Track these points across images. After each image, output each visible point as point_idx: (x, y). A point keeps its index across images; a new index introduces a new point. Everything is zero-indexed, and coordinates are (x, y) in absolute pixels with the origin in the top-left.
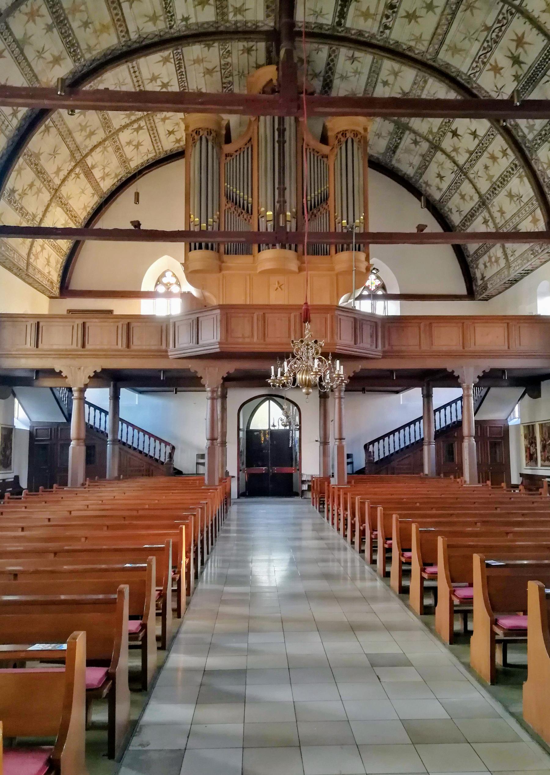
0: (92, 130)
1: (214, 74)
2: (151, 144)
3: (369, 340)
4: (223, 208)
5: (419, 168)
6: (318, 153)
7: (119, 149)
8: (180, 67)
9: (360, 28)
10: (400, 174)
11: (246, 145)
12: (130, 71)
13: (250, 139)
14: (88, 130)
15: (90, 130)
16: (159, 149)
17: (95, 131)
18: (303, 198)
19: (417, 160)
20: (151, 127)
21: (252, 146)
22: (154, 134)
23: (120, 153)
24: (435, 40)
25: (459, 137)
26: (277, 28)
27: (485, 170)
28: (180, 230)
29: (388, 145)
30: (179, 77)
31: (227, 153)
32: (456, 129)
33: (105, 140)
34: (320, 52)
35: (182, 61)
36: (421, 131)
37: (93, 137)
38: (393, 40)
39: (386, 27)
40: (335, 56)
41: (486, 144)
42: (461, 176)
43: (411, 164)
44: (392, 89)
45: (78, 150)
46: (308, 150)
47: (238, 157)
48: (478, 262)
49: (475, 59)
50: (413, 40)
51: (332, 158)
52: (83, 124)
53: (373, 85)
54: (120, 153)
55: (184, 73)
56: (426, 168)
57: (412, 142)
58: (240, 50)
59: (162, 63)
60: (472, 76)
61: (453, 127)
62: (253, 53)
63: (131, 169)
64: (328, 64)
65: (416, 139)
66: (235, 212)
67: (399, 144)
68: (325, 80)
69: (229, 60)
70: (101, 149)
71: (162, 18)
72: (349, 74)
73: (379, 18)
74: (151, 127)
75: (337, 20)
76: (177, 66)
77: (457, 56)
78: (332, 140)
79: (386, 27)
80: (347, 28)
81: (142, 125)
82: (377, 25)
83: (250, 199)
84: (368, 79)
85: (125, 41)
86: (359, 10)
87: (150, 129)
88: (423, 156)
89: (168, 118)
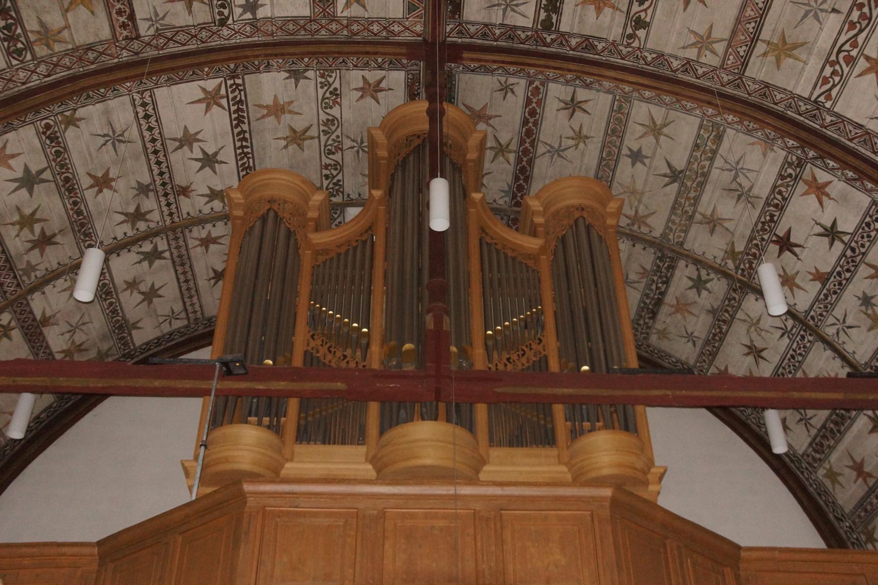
0: (48, 233)
1: (307, 143)
5: (707, 342)
7: (108, 293)
8: (240, 121)
9: (587, 32)
14: (37, 228)
15: (43, 231)
16: (195, 312)
19: (700, 325)
20: (180, 256)
22: (184, 273)
23: (111, 304)
25: (796, 250)
27: (863, 308)
30: (238, 144)
32: (789, 232)
35: (244, 107)
37: (49, 249)
38: (651, 52)
39: (640, 24)
40: (539, 103)
41: (863, 246)
42: (803, 337)
43: (690, 337)
45: (11, 269)
48: (870, 528)
49: (830, 55)
52: (28, 211)
54: (111, 304)
55: (247, 135)
56: (722, 340)
57: (691, 284)
59: (203, 106)
60: (822, 99)
61: (781, 232)
63: (135, 350)
64: (525, 122)
65: (699, 276)
67: (663, 294)
68: (519, 160)
69: (335, 111)
75: (543, 15)
79: (640, 24)
80: (563, 35)
81: (160, 249)
82: (620, 18)
84: (602, 151)
85: (126, 38)
87: (177, 260)
88: (713, 312)
89: (215, 241)
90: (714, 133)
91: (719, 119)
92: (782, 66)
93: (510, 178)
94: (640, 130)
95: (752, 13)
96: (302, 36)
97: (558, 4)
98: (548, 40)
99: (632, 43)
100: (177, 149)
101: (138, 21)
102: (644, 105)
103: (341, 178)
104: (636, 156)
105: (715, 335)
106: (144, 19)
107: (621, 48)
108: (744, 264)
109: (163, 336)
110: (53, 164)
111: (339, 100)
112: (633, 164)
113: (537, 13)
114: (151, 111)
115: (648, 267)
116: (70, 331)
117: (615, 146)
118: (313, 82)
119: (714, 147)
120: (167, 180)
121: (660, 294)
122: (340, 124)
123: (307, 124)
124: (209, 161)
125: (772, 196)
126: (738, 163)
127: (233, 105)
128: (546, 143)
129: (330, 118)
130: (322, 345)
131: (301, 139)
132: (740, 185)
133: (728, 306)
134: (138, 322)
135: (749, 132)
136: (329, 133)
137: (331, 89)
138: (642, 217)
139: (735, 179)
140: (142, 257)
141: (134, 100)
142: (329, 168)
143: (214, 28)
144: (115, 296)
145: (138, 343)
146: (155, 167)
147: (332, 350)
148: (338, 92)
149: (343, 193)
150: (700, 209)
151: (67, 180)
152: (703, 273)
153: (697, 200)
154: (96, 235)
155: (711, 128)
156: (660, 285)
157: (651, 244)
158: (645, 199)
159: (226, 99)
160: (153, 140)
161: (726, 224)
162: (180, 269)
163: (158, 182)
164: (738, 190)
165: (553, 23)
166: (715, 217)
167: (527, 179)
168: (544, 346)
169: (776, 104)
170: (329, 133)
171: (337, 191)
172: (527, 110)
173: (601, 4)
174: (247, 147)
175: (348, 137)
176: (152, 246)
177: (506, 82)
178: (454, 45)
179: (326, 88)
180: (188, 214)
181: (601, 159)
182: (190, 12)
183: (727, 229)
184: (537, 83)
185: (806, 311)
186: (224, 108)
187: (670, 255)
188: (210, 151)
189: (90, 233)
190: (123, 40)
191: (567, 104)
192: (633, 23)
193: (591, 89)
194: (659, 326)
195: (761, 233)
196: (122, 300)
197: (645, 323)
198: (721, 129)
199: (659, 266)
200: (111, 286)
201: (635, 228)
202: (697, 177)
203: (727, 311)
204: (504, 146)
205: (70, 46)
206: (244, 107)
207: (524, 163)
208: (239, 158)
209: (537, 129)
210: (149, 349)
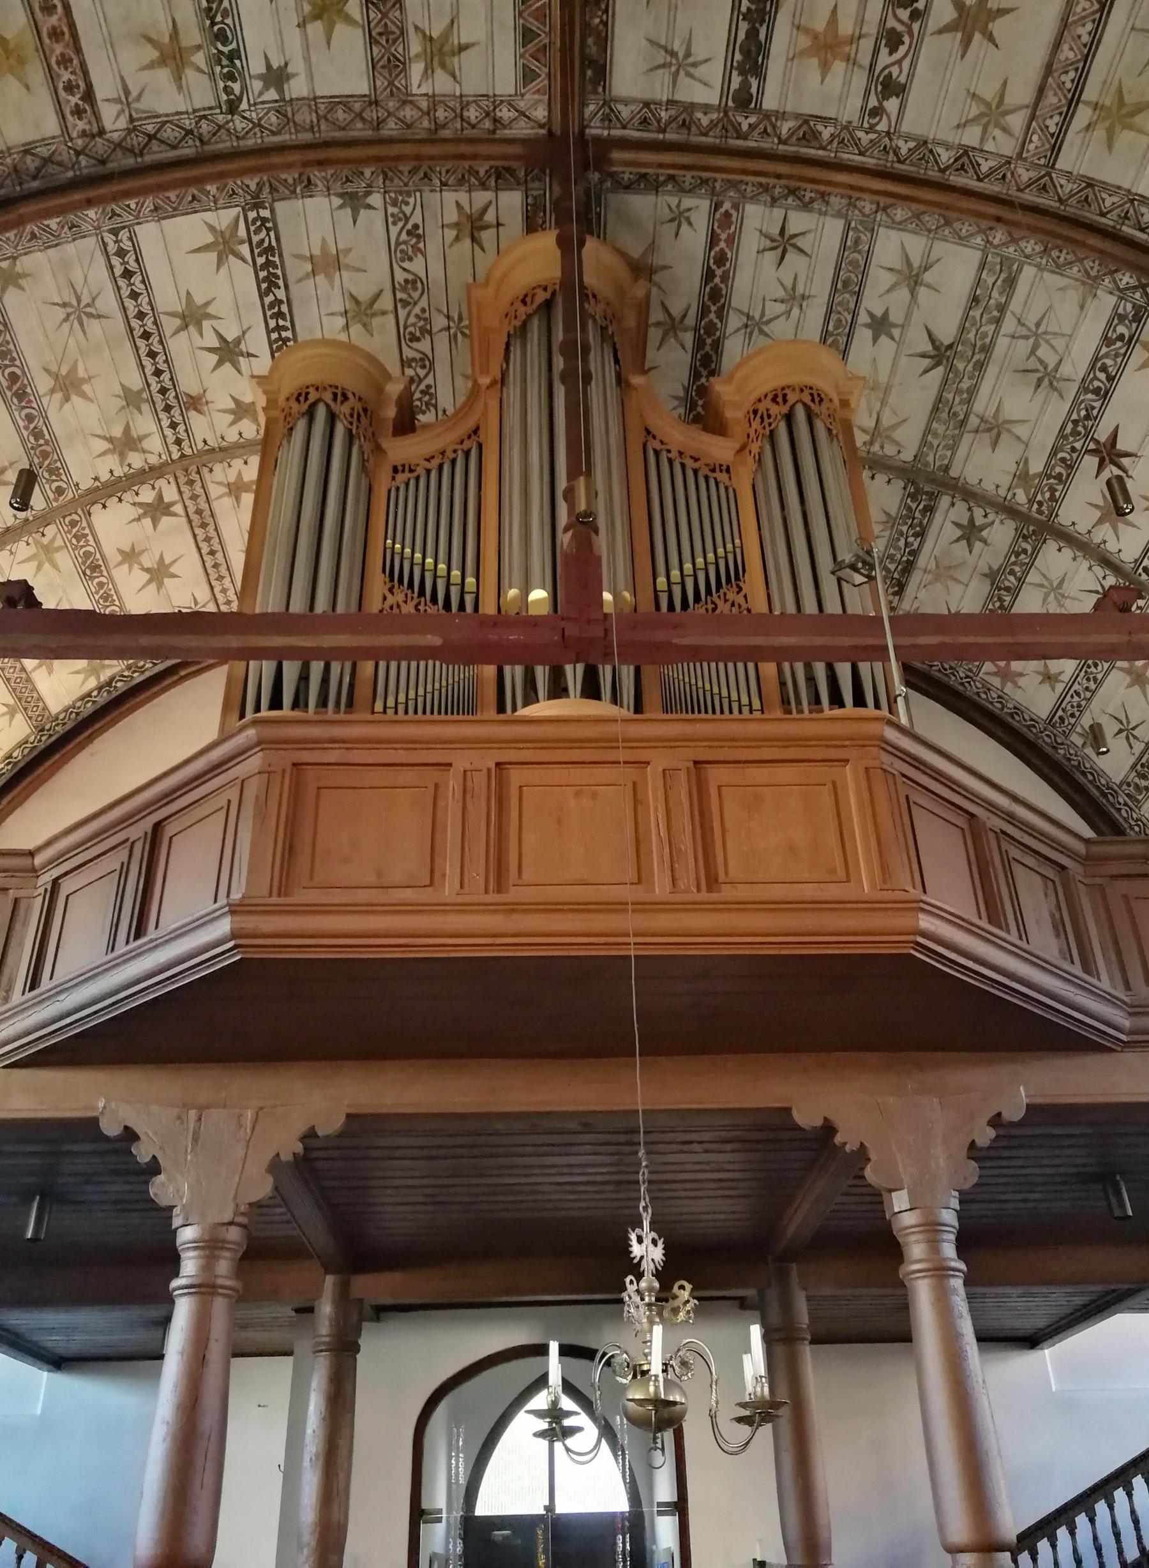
1: (376, 321)
6: (696, 460)
7: (95, 568)
9: (807, 109)
11: (462, 442)
20: (199, 512)
21: (480, 446)
22: (208, 539)
23: (101, 585)
24: (1051, 99)
26: (557, 129)
30: (272, 323)
31: (399, 464)
34: (685, 227)
35: (277, 259)
36: (989, 486)
40: (730, 241)
46: (664, 456)
50: (974, 120)
54: (101, 585)
58: (449, 226)
61: (1102, 434)
62: (487, 236)
64: (709, 275)
65: (972, 520)
67: (915, 553)
68: (699, 344)
69: (417, 266)
70: (32, 550)
71: (199, 59)
73: (866, 46)
76: (263, 274)
77: (1125, 137)
79: (891, 87)
80: (767, 116)
81: (166, 499)
82: (860, 80)
83: (470, 580)
85: (84, 134)
86: (807, 31)
87: (195, 518)
88: (993, 576)
90: (1003, 276)
91: (1011, 249)
92: (1117, 145)
93: (684, 374)
94: (888, 279)
95: (1071, 55)
96: (359, 131)
97: (760, 59)
98: (745, 127)
99: (877, 124)
101: (99, 102)
102: (894, 234)
104: (880, 325)
106: (107, 100)
107: (860, 134)
108: (1043, 494)
111: (421, 245)
112: (875, 339)
113: (727, 80)
115: (893, 513)
117: (847, 310)
118: (382, 213)
120: (168, 384)
121: (910, 553)
122: (426, 289)
123: (374, 290)
125: (1092, 375)
126: (1038, 325)
127: (260, 255)
128: (740, 311)
129: (410, 277)
130: (406, 602)
131: (367, 315)
132: (1041, 361)
133: (1014, 563)
135: (1059, 269)
136: (409, 303)
137: (409, 226)
138: (887, 429)
139: (1033, 352)
140: (141, 511)
141: (105, 245)
142: (414, 364)
143: (220, 117)
144: (105, 573)
146: (147, 362)
148: (420, 231)
149: (435, 406)
150: (978, 406)
152: (978, 513)
153: (972, 391)
154: (68, 473)
155: (998, 267)
156: (911, 539)
158: (892, 399)
159: (247, 245)
161: (1018, 430)
163: (155, 387)
164: (1037, 371)
165: (751, 95)
168: (745, 596)
169: (1103, 215)
170: (409, 303)
171: (427, 404)
172: (712, 254)
173: (829, 56)
174: (285, 329)
175: (439, 311)
177: (678, 206)
178: (597, 139)
179: (400, 224)
180: (205, 442)
182: (180, 88)
183: (1018, 438)
184: (727, 206)
185: (1136, 561)
187: (926, 489)
189: (58, 469)
190: (79, 137)
191: (773, 240)
192: (880, 88)
193: (810, 211)
195: (1071, 439)
196: (117, 580)
198: (1015, 267)
199: (909, 509)
200: (98, 556)
201: (876, 448)
202: (973, 354)
203: (1012, 572)
204: (677, 320)
206: (277, 259)
207: (708, 348)
208: (274, 346)
209: (727, 287)
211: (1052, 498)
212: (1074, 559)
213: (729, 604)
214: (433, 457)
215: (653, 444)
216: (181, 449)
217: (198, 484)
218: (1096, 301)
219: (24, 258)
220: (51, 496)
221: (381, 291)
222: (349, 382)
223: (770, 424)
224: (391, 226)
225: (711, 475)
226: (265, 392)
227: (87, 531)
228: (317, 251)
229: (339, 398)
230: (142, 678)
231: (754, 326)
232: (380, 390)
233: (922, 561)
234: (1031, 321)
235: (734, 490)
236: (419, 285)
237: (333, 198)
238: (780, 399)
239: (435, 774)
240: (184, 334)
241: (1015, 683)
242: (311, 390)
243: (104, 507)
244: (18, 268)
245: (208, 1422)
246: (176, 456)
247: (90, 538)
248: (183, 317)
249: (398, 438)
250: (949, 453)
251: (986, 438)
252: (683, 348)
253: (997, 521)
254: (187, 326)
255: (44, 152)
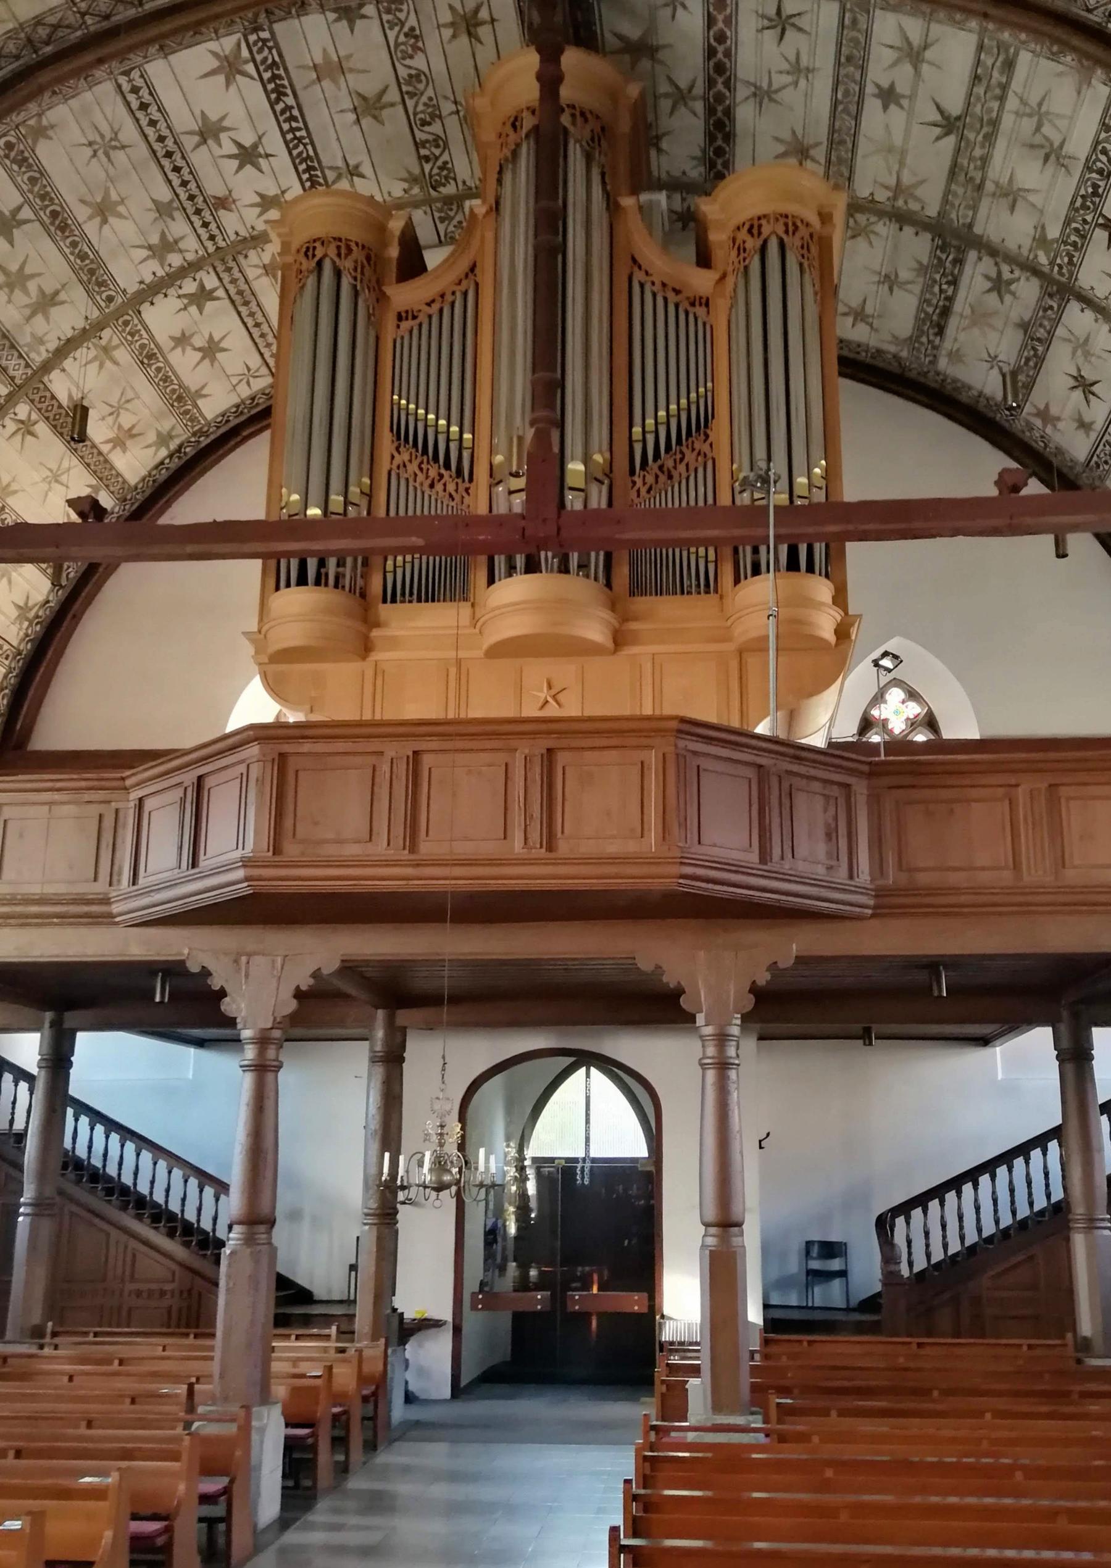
0: (49, 290)
1: (385, 113)
2: (254, 349)
3: (821, 849)
4: (384, 465)
6: (677, 292)
7: (151, 356)
8: (280, 94)
10: (964, 398)
11: (460, 283)
12: (128, 104)
13: (473, 269)
15: (41, 291)
17: (57, 293)
18: (631, 426)
20: (240, 293)
21: (477, 284)
22: (252, 314)
23: (159, 370)
28: (219, 519)
29: (920, 309)
30: (286, 127)
31: (402, 309)
33: (98, 327)
35: (282, 72)
36: (1011, 245)
37: (54, 311)
40: (728, 21)
44: (910, 113)
45: (13, 347)
46: (648, 288)
47: (435, 320)
51: (721, 306)
53: (853, 108)
54: (159, 370)
55: (296, 112)
56: (1038, 367)
57: (988, 285)
58: (445, 26)
59: (221, 79)
62: (484, 32)
63: (209, 424)
64: (711, 52)
65: (999, 273)
66: (421, 477)
67: (950, 299)
68: (710, 111)
69: (419, 62)
70: (93, 353)
72: (779, 80)
74: (240, 293)
76: (271, 86)
78: (722, 255)
83: (467, 436)
84: (835, 90)
88: (1024, 326)
100: (197, 146)
103: (448, 159)
104: (888, 96)
105: (1028, 360)
109: (243, 402)
110: (31, 196)
112: (885, 107)
114: (147, 98)
115: (925, 261)
116: (111, 414)
117: (855, 82)
118: (377, 22)
119: (1004, 80)
120: (195, 191)
122: (430, 80)
123: (379, 87)
124: (248, 156)
125: (1094, 157)
127: (266, 70)
129: (413, 72)
134: (203, 387)
137: (406, 29)
140: (186, 301)
141: (119, 86)
144: (161, 359)
145: (210, 416)
146: (173, 176)
147: (424, 466)
148: (418, 32)
149: (455, 179)
151: (54, 215)
153: (985, 160)
156: (945, 287)
157: (922, 225)
158: (909, 160)
160: (161, 139)
161: (1032, 198)
162: (244, 310)
163: (183, 196)
166: (1015, 188)
167: (729, 137)
168: (711, 445)
170: (415, 94)
171: (446, 178)
172: (712, 33)
174: (299, 129)
175: (446, 98)
176: (195, 285)
179: (397, 29)
180: (237, 234)
181: (835, 104)
183: (1033, 205)
186: (252, 78)
188: (248, 142)
189: (105, 281)
194: (948, 345)
197: (929, 342)
199: (939, 259)
200: (152, 346)
201: (900, 203)
203: (1041, 325)
205: (11, 26)
206: (282, 72)
208: (291, 145)
210: (228, 421)
211: (1071, 262)
212: (1096, 320)
213: (696, 453)
214: (433, 301)
215: (639, 276)
216: (215, 244)
217: (235, 271)
218: (1090, 91)
219: (48, 113)
220: (103, 304)
221: (387, 87)
222: (353, 234)
223: (744, 260)
224: (388, 31)
225: (691, 310)
226: (279, 235)
227: (139, 327)
228: (319, 60)
229: (343, 251)
230: (209, 441)
231: (763, 95)
232: (381, 229)
233: (958, 306)
234: (1033, 101)
235: (712, 327)
236: (423, 77)
237: (327, 13)
238: (755, 231)
239: (371, 760)
240: (204, 148)
241: (1055, 426)
242: (317, 244)
243: (152, 304)
244: (45, 122)
245: (268, 1143)
246: (211, 248)
247: (143, 332)
248: (201, 134)
249: (402, 284)
250: (970, 213)
251: (1005, 203)
252: (695, 114)
253: (1023, 279)
254: (205, 141)
255: (52, 20)
